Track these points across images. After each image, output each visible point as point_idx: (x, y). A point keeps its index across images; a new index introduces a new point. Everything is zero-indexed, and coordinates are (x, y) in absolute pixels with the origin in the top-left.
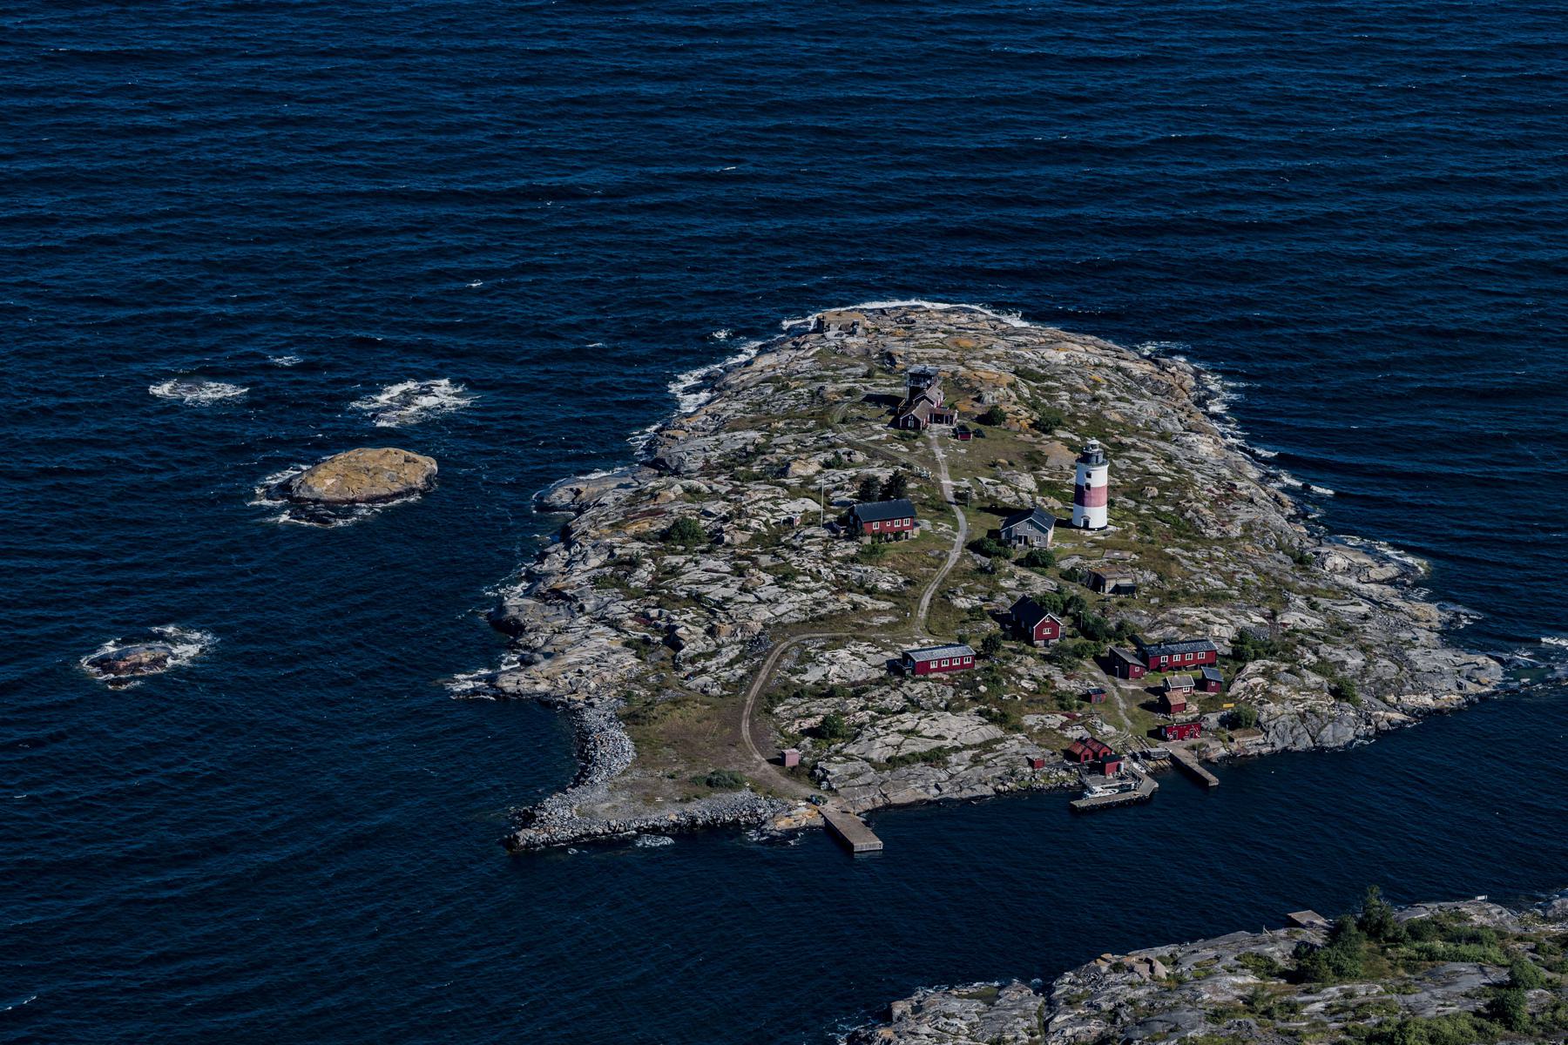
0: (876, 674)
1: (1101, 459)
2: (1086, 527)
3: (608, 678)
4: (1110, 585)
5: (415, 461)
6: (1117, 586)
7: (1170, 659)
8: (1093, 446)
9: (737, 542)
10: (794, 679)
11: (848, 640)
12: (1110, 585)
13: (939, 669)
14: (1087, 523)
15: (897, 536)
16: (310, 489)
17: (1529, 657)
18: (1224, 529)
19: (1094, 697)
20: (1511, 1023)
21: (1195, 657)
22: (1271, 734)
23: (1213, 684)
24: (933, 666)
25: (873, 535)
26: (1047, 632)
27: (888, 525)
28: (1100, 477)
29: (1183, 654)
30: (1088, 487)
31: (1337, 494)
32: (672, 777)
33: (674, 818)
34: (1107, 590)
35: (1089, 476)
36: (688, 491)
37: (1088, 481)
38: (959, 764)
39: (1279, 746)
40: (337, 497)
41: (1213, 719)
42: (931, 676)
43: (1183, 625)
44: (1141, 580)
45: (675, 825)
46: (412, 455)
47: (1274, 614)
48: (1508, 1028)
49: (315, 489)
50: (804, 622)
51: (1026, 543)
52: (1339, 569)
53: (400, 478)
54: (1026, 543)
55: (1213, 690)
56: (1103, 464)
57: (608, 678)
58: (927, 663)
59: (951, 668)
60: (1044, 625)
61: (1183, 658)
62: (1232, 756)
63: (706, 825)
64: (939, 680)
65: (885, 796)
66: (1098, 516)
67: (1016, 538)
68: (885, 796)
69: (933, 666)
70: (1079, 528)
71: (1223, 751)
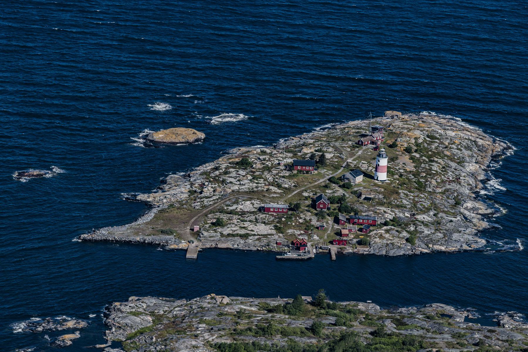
0: (254, 210)
1: (384, 156)
2: (377, 180)
3: (172, 200)
4: (363, 197)
5: (196, 134)
6: (365, 197)
7: (358, 221)
8: (382, 151)
9: (257, 168)
10: (225, 208)
11: (255, 199)
12: (363, 197)
13: (274, 212)
14: (377, 178)
15: (307, 172)
16: (153, 137)
17: (135, 142)
18: (435, 189)
19: (320, 228)
20: (314, 332)
21: (368, 222)
22: (372, 248)
23: (364, 230)
24: (272, 210)
25: (298, 170)
26: (321, 206)
27: (304, 168)
28: (384, 162)
29: (363, 220)
30: (379, 165)
31: (507, 190)
32: (153, 228)
33: (138, 239)
34: (362, 198)
35: (379, 161)
36: (262, 152)
37: (379, 163)
38: (250, 240)
39: (372, 252)
40: (160, 141)
41: (355, 241)
42: (270, 213)
43: (376, 212)
44: (377, 197)
45: (138, 241)
46: (196, 131)
47: (414, 215)
48: (314, 334)
49: (154, 137)
50: (247, 192)
51: (349, 180)
52: (469, 208)
53: (186, 138)
54: (349, 180)
55: (364, 232)
56: (386, 158)
57: (172, 200)
58: (270, 208)
59: (278, 212)
60: (320, 203)
61: (363, 221)
62: (354, 253)
63: (148, 243)
64: (272, 215)
65: (217, 245)
66: (383, 176)
67: (346, 178)
68: (217, 245)
69: (272, 210)
70: (375, 179)
71: (351, 251)
